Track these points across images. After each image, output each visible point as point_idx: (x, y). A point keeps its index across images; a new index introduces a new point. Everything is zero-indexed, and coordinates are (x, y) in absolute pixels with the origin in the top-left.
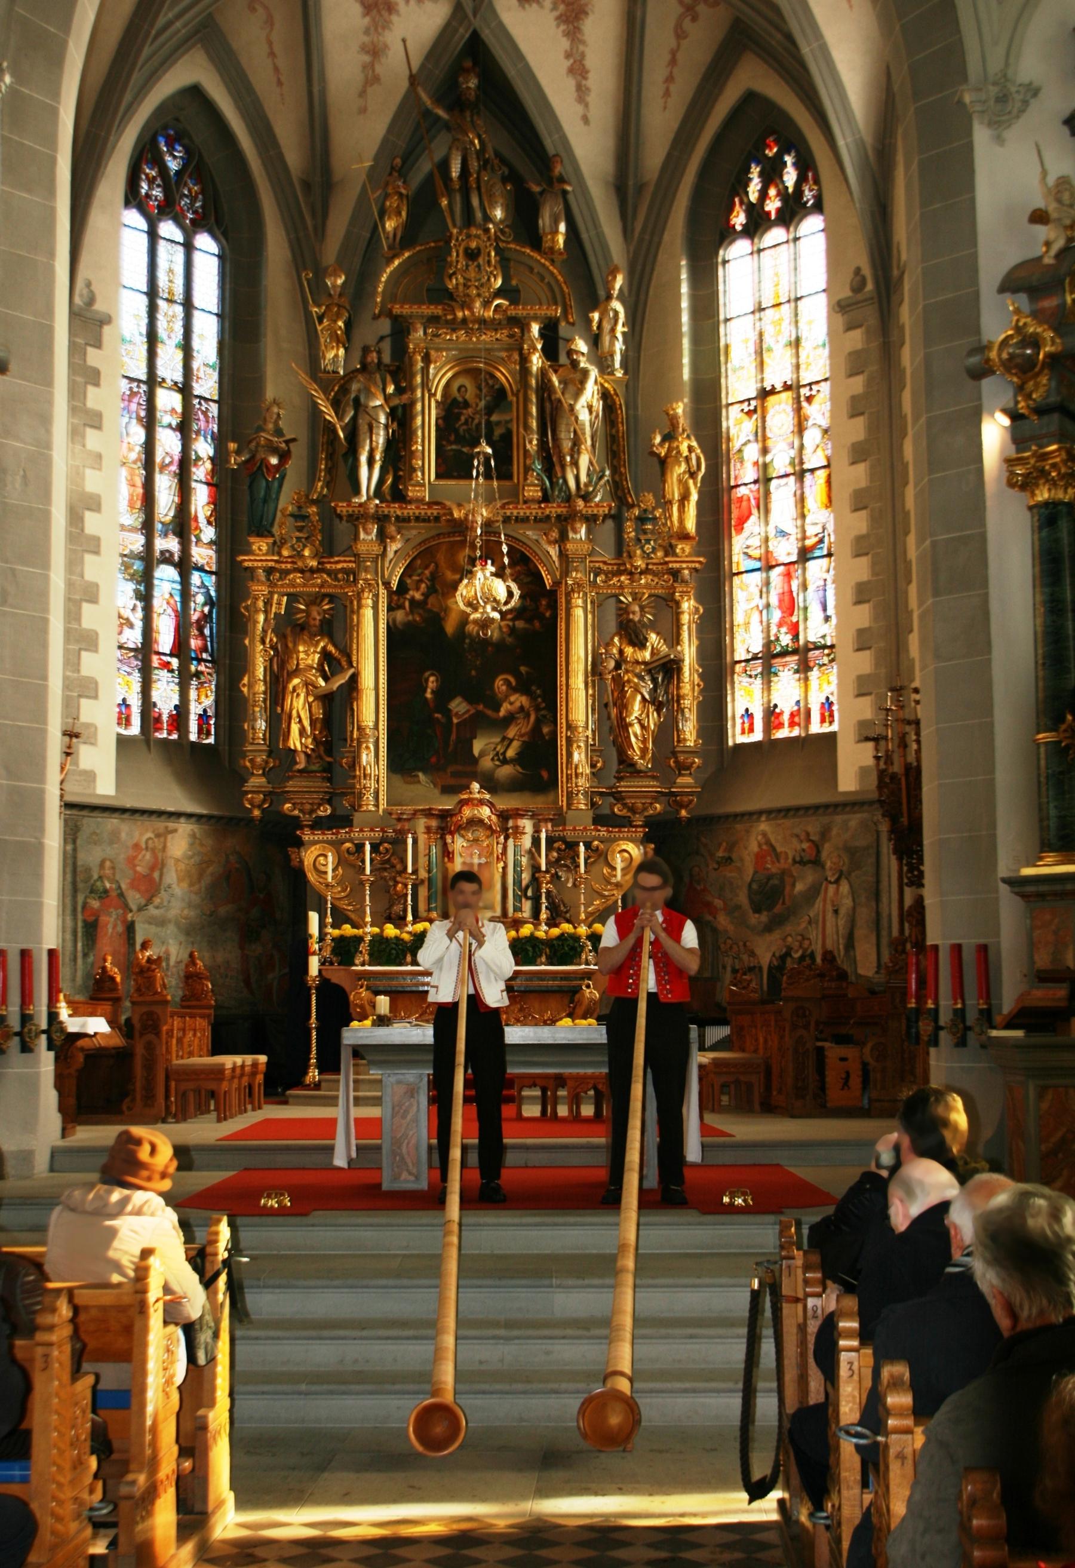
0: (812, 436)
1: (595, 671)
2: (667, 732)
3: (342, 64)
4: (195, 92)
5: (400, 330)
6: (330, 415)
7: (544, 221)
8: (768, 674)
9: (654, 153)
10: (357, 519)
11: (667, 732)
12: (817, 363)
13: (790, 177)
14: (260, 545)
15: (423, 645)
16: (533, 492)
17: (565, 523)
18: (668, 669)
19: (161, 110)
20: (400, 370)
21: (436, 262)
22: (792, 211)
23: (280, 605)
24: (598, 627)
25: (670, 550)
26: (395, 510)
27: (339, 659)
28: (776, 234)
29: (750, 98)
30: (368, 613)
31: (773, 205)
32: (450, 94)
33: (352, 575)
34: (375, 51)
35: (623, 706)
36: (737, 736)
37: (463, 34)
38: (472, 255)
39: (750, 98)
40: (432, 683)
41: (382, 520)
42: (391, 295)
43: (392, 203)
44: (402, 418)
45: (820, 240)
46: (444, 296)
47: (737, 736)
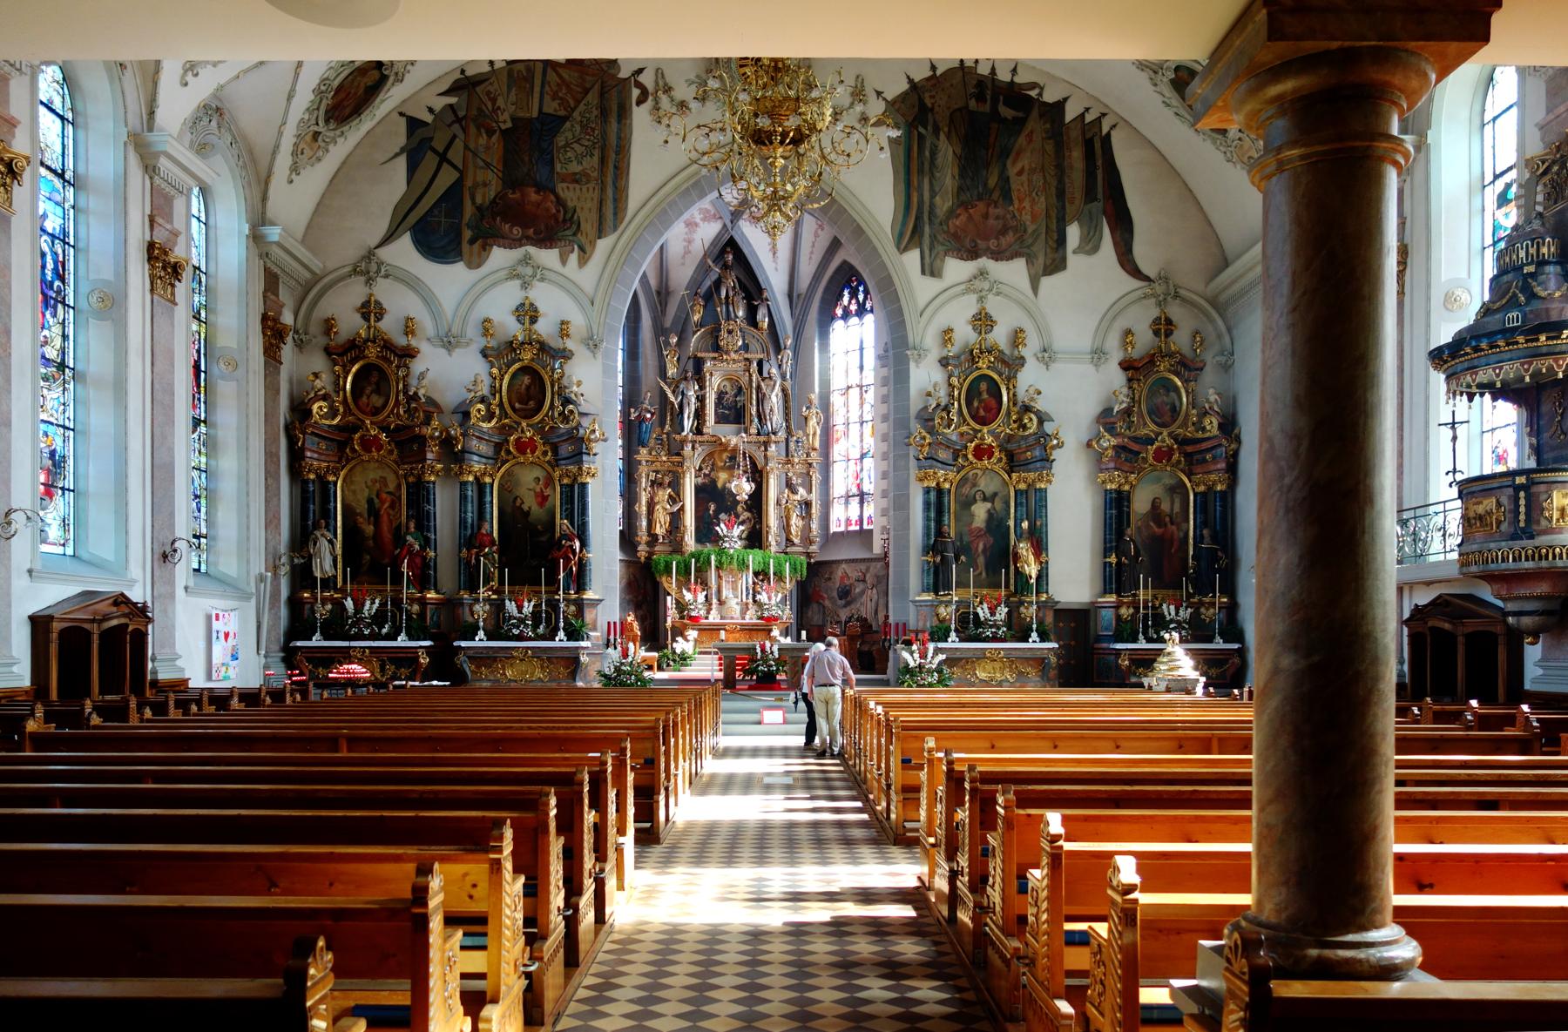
0: (867, 407)
1: (778, 503)
2: (807, 529)
5: (699, 363)
6: (672, 398)
7: (759, 317)
8: (847, 503)
9: (804, 281)
10: (683, 442)
11: (807, 529)
12: (869, 377)
13: (861, 297)
14: (644, 451)
15: (709, 493)
16: (753, 431)
17: (766, 444)
18: (807, 504)
20: (698, 373)
21: (715, 334)
22: (861, 311)
23: (652, 476)
24: (779, 485)
25: (808, 455)
26: (699, 438)
27: (676, 498)
28: (854, 320)
29: (845, 262)
30: (687, 480)
31: (853, 307)
32: (719, 257)
33: (681, 464)
35: (788, 518)
36: (834, 528)
37: (726, 237)
38: (730, 332)
39: (845, 262)
40: (712, 507)
41: (694, 442)
42: (696, 349)
43: (697, 308)
44: (701, 399)
45: (873, 326)
46: (717, 348)
47: (834, 528)
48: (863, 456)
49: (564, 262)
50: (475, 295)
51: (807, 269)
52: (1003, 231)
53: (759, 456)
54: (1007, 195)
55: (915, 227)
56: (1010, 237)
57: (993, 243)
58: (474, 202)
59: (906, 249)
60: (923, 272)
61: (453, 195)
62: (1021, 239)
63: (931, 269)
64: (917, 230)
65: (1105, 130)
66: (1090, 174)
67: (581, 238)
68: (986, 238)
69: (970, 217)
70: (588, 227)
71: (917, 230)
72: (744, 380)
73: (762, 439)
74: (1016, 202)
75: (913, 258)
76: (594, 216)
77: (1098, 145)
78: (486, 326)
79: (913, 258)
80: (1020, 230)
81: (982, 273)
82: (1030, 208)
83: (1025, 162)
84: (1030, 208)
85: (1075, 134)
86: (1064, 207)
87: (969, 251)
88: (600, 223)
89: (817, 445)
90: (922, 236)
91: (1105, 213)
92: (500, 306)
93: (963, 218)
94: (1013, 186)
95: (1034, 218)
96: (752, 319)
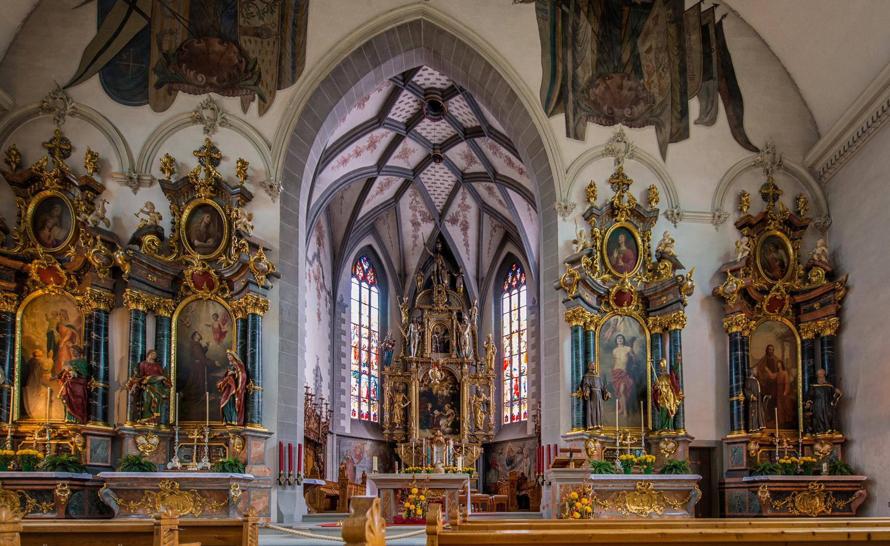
3: (408, 241)
4: (370, 246)
19: (361, 250)
34: (416, 237)
48: (521, 374)
49: (245, 110)
50: (158, 137)
51: (487, 260)
52: (636, 101)
53: (457, 372)
54: (638, 69)
55: (558, 96)
56: (641, 108)
57: (627, 112)
58: (160, 45)
59: (550, 114)
60: (568, 135)
61: (142, 40)
62: (650, 109)
63: (575, 133)
64: (562, 97)
65: (717, 19)
66: (707, 56)
67: (262, 88)
68: (622, 107)
69: (607, 88)
70: (268, 78)
71: (562, 97)
72: (448, 325)
73: (459, 360)
74: (646, 76)
75: (559, 120)
76: (274, 70)
77: (712, 31)
78: (170, 164)
79: (559, 120)
80: (650, 101)
81: (619, 138)
82: (657, 81)
83: (652, 42)
84: (657, 81)
85: (693, 20)
86: (685, 83)
87: (607, 117)
88: (280, 75)
89: (493, 367)
90: (566, 102)
91: (719, 90)
92: (184, 149)
93: (602, 87)
94: (643, 62)
95: (661, 92)
96: (453, 285)
